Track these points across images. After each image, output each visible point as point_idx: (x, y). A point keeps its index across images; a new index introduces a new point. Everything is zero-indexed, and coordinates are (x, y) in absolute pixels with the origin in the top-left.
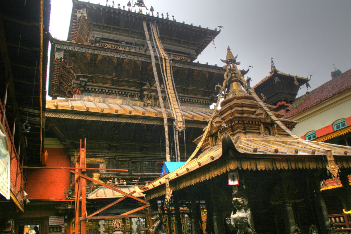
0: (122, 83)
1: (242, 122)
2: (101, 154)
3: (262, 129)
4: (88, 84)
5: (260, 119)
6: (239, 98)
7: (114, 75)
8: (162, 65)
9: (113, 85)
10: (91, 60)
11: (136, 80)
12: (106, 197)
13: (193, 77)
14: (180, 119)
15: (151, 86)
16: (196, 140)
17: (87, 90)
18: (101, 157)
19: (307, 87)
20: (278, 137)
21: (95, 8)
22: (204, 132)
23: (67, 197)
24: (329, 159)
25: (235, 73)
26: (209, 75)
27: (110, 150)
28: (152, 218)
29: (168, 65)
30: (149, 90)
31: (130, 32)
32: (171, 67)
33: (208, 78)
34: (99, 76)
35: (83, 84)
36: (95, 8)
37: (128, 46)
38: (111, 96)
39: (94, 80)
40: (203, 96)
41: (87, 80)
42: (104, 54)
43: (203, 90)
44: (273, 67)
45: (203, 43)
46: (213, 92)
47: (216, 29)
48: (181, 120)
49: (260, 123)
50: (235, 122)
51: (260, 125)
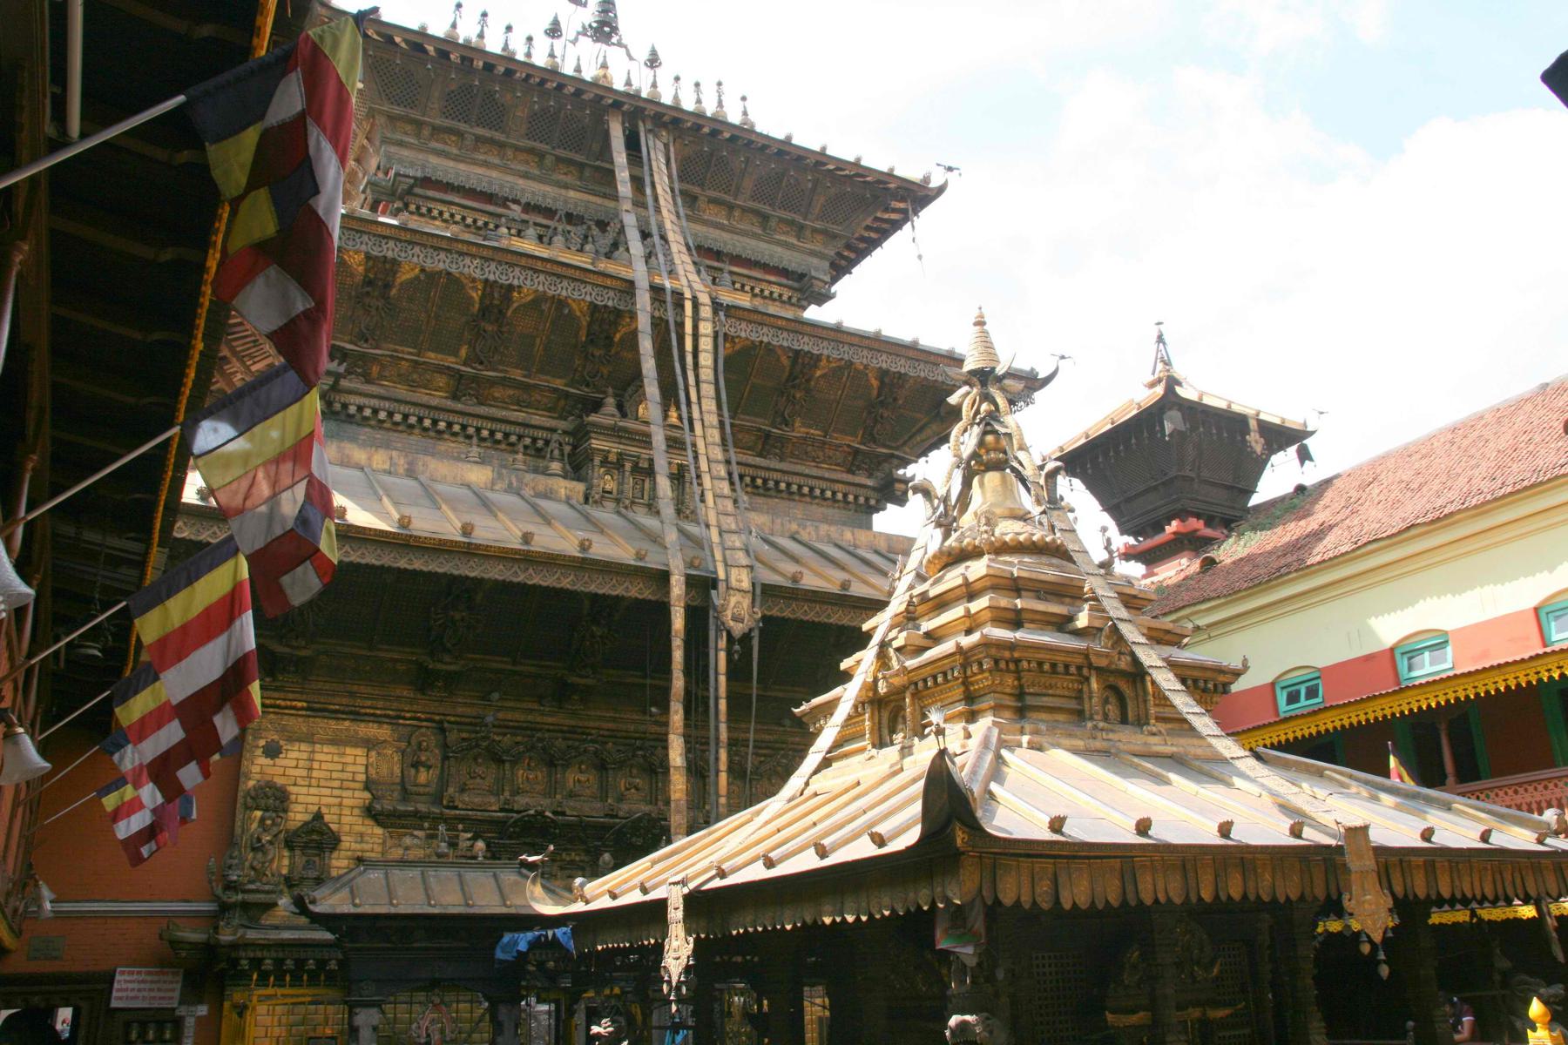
0: (498, 393)
1: (1012, 666)
2: (380, 704)
3: (1090, 698)
4: (344, 383)
5: (1085, 654)
6: (1002, 549)
7: (463, 352)
8: (680, 325)
11: (559, 383)
12: (393, 910)
14: (741, 579)
15: (624, 415)
16: (805, 707)
17: (337, 413)
18: (377, 719)
19: (1302, 464)
21: (403, 45)
22: (846, 677)
23: (219, 891)
25: (995, 432)
26: (882, 382)
27: (422, 690)
28: (595, 1029)
29: (706, 328)
30: (616, 433)
31: (549, 161)
32: (721, 339)
33: (875, 393)
36: (403, 45)
37: (536, 224)
38: (443, 446)
39: (375, 369)
40: (850, 471)
41: (342, 369)
42: (429, 261)
44: (1163, 361)
45: (868, 228)
46: (892, 456)
47: (927, 179)
48: (746, 585)
49: (1085, 671)
50: (980, 664)
51: (1087, 679)
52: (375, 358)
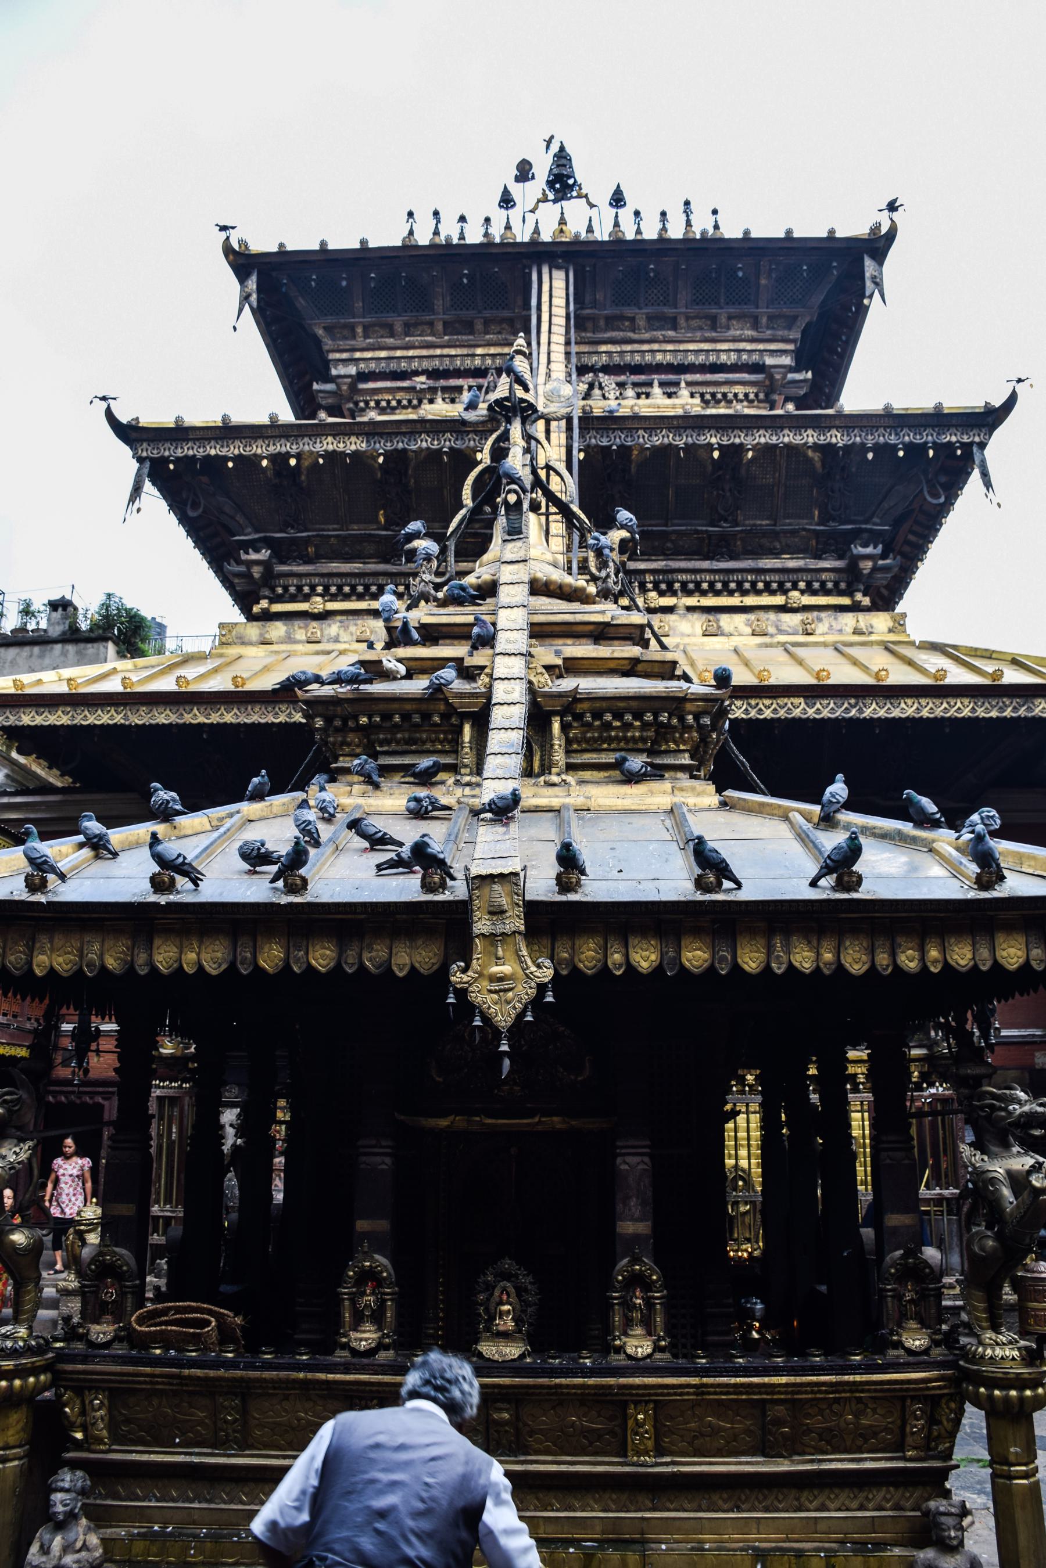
9: (386, 561)
10: (278, 474)
13: (743, 471)
20: (554, 785)
24: (482, 925)
33: (818, 465)
34: (324, 530)
35: (257, 572)
43: (804, 529)
46: (860, 531)
51: (460, 732)
52: (307, 541)
